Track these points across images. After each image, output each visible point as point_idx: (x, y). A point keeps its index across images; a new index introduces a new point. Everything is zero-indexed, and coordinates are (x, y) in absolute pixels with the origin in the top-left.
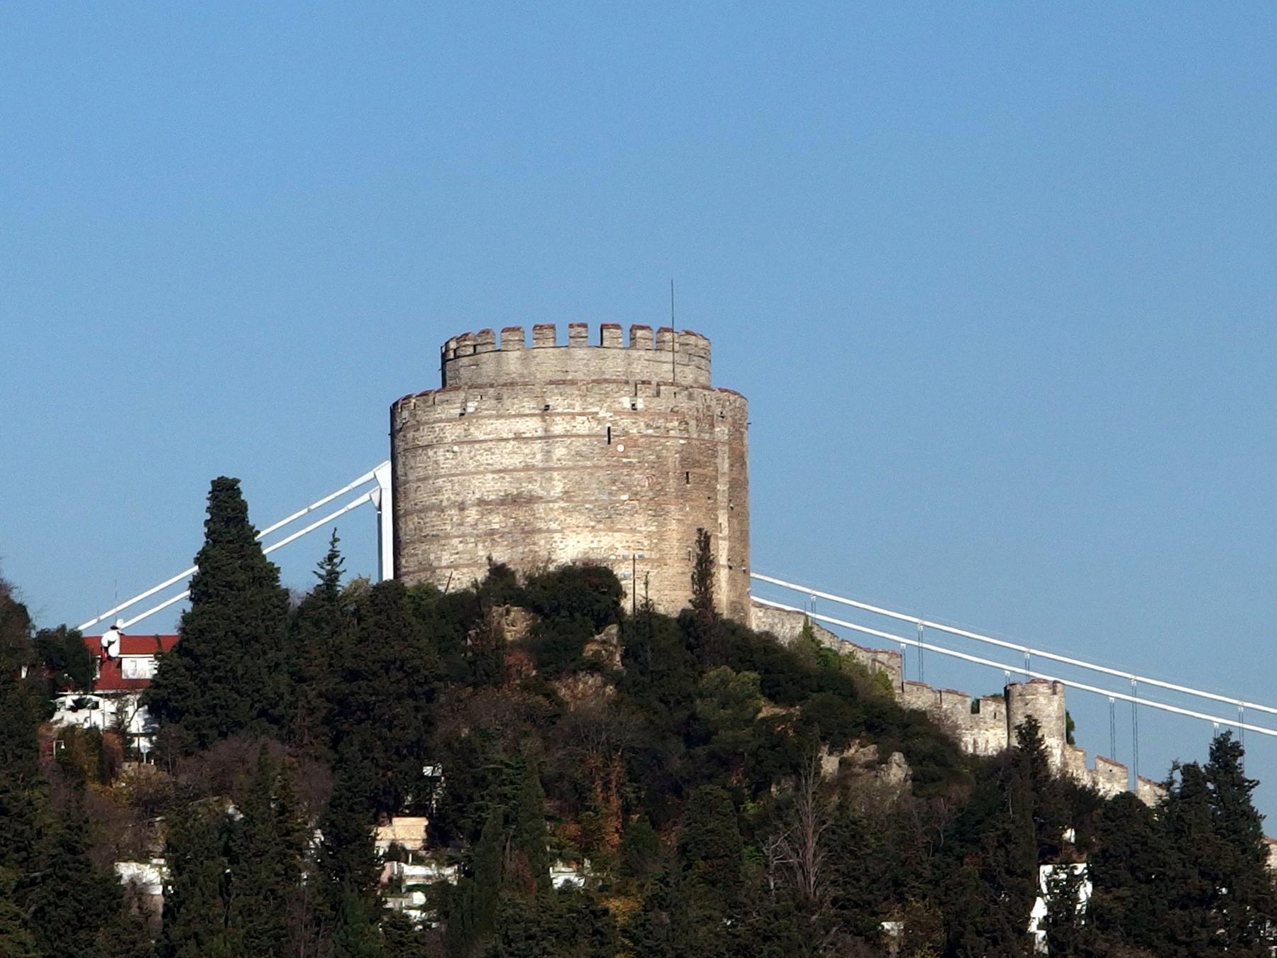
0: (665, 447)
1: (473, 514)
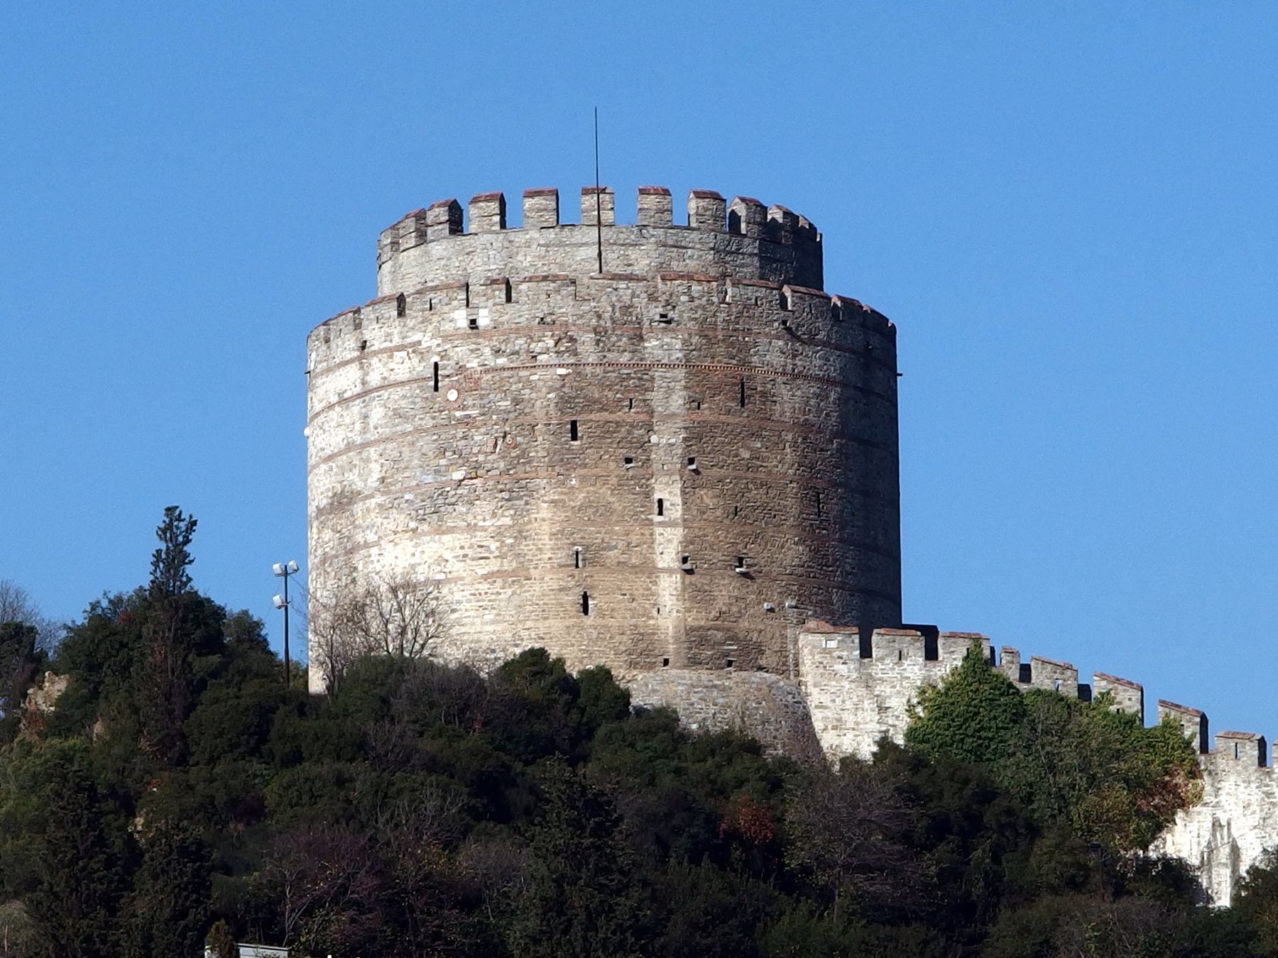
0: (528, 384)
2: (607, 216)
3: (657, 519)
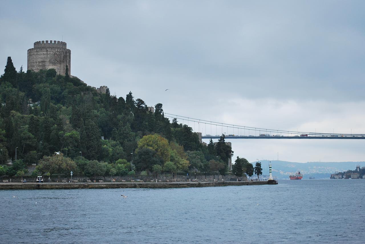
1: (38, 63)
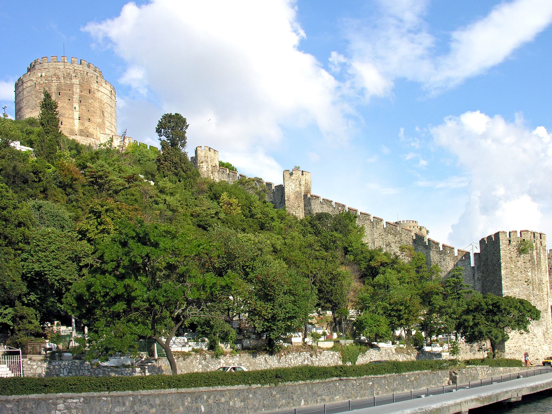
2: (66, 61)
3: (74, 110)
